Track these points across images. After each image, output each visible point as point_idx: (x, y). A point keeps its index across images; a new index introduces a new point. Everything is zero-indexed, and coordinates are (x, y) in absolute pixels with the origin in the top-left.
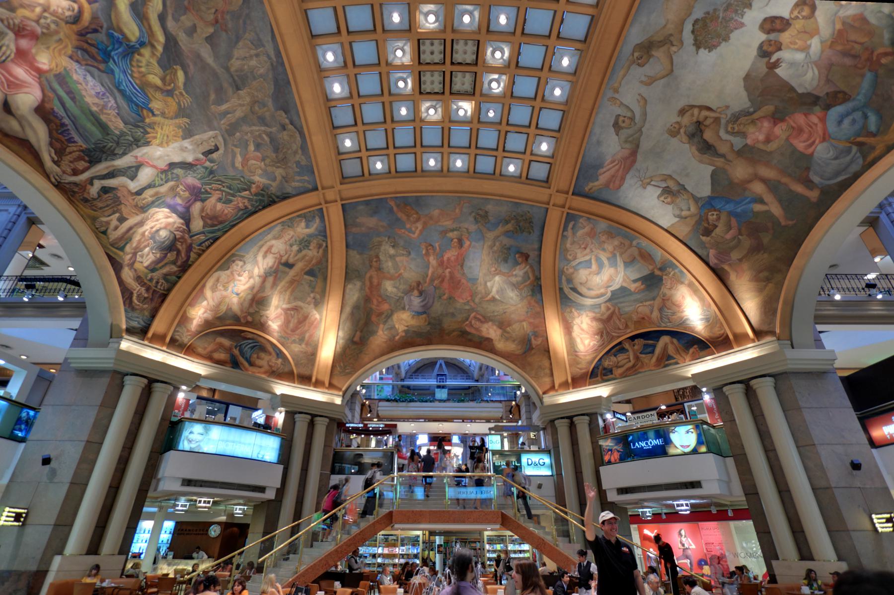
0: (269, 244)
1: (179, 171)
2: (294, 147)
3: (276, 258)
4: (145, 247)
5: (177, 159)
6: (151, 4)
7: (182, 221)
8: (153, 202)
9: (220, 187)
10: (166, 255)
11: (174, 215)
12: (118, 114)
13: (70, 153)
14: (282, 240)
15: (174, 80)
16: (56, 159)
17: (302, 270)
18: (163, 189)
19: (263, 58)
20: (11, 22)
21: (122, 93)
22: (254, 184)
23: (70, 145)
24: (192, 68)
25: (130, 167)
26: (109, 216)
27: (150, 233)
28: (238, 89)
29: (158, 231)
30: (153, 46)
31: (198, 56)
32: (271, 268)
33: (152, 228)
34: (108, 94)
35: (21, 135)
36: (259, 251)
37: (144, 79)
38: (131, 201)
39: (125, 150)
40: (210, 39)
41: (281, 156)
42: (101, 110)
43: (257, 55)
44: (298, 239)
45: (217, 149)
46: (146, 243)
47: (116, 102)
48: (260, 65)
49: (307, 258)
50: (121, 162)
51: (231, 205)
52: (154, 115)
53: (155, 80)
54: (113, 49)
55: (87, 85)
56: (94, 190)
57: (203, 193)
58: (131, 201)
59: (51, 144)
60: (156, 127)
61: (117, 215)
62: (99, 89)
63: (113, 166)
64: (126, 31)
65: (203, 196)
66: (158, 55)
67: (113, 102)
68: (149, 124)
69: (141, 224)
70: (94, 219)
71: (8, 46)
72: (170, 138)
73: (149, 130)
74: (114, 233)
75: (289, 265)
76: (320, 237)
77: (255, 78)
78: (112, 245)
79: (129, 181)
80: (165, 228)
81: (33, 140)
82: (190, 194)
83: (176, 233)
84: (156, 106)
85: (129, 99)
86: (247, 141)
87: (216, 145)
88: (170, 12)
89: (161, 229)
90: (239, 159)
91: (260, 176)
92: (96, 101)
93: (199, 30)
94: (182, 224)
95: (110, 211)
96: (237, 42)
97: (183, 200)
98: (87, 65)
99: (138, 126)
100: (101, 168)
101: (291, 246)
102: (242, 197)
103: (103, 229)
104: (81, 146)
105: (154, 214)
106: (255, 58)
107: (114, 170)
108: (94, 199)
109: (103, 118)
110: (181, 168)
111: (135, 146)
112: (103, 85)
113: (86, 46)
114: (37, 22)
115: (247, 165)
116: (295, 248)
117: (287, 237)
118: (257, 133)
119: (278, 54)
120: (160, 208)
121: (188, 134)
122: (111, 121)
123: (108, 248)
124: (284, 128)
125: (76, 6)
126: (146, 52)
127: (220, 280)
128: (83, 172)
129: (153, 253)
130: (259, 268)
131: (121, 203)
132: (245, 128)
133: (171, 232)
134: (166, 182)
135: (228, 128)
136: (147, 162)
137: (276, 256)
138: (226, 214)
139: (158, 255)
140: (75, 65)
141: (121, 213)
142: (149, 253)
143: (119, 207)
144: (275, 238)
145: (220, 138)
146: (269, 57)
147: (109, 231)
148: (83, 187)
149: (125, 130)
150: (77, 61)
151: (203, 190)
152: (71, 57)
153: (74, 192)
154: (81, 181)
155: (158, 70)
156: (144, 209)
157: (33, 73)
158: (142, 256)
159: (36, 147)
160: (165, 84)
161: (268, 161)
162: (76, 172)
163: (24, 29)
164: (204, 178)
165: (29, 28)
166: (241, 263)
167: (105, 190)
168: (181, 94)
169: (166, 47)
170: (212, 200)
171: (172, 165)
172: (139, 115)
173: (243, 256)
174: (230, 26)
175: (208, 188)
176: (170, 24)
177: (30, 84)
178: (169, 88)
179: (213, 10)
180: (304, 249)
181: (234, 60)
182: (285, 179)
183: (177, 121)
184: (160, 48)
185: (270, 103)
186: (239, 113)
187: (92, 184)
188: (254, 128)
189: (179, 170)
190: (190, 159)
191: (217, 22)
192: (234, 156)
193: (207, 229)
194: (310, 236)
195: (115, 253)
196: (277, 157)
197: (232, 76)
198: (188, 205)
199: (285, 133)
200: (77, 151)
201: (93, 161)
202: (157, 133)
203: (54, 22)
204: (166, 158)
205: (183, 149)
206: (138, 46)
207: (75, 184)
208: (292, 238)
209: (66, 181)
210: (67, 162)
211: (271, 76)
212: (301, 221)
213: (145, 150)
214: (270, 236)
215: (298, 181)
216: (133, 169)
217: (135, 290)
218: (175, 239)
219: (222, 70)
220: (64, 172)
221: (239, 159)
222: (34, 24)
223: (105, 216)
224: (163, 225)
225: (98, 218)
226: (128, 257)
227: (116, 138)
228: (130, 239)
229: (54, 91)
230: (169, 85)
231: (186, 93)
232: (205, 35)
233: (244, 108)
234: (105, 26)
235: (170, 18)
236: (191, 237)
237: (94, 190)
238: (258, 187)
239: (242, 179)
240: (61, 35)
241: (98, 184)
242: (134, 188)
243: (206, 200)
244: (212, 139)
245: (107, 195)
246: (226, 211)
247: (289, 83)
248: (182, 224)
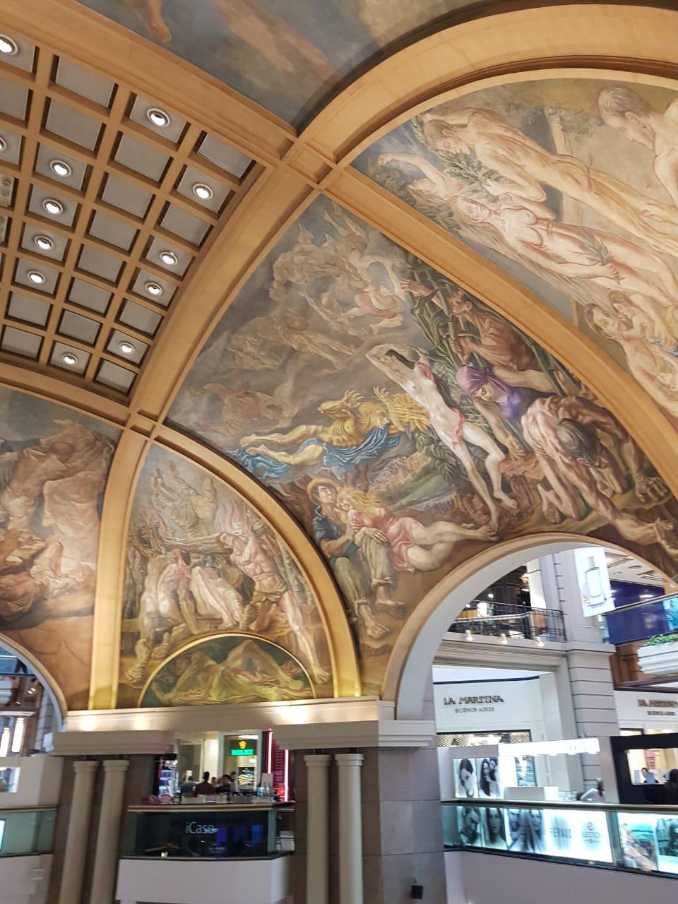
0: (521, 249)
1: (455, 395)
2: (298, 259)
3: (549, 233)
4: (589, 474)
5: (438, 398)
6: (279, 442)
7: (537, 402)
8: (514, 435)
9: (451, 341)
10: (602, 446)
11: (529, 411)
12: (407, 457)
13: (465, 509)
14: (493, 220)
15: (339, 411)
16: (472, 525)
17: (545, 162)
18: (492, 420)
19: (234, 342)
20: (354, 527)
21: (381, 453)
22: (411, 294)
23: (456, 506)
24: (312, 398)
25: (469, 450)
26: (541, 498)
27: (566, 456)
28: (293, 351)
29: (560, 442)
30: (315, 433)
31: (294, 397)
32: (582, 246)
33: (557, 450)
34: (389, 464)
35: (451, 546)
36: (551, 272)
37: (354, 435)
38: (518, 463)
39: (449, 454)
40: (269, 391)
41: (331, 270)
42: (410, 471)
43: (240, 350)
44: (467, 187)
45: (391, 353)
46: (583, 470)
47: (395, 457)
48: (247, 343)
49: (501, 152)
50: (467, 462)
51: (477, 322)
52: (391, 423)
53: (349, 426)
54: (341, 461)
55: (387, 481)
56: (508, 502)
57: (476, 363)
58: (518, 463)
59: (459, 523)
60: (406, 421)
61: (540, 487)
62: (386, 470)
63: (473, 471)
64: (317, 454)
65: (482, 366)
66: (320, 428)
67: (395, 460)
68: (405, 427)
69: (551, 462)
70: (543, 520)
71: (375, 533)
72: (411, 406)
73: (413, 428)
74: (564, 505)
75: (553, 200)
76: (420, 136)
77: (265, 341)
78: (581, 518)
79: (489, 457)
80: (555, 430)
81: (454, 538)
82: (487, 382)
83: (561, 417)
84: (379, 421)
85: (385, 447)
86: (350, 320)
87: (387, 354)
88: (273, 428)
89: (557, 437)
90: (385, 322)
91: (391, 288)
92: (400, 473)
93: (270, 403)
94: (543, 403)
95: (535, 494)
96: (247, 371)
97: (500, 395)
98: (367, 480)
99: (413, 437)
100: (479, 484)
101: (495, 199)
102: (449, 307)
103: (557, 515)
104: (456, 497)
105: (533, 439)
106: (245, 350)
107: (478, 471)
108: (519, 506)
109: (418, 471)
110: (449, 394)
111: (440, 444)
112: (381, 469)
113: (349, 481)
114: (347, 511)
115: (387, 310)
116: (494, 188)
117: (480, 214)
118: (329, 311)
119: (215, 335)
120: (522, 428)
121: (393, 388)
122: (418, 463)
123: (585, 526)
124: (288, 285)
125: (320, 487)
126: (326, 437)
127: (649, 371)
128: (485, 504)
129: (600, 467)
130: (595, 277)
131: (523, 476)
132: (335, 327)
133: (561, 423)
134: (479, 413)
135: (352, 346)
136: (457, 432)
137: (544, 234)
138: (498, 330)
139: (605, 461)
140: (371, 488)
141: (539, 482)
142: (599, 472)
143: (529, 481)
144: (498, 237)
145: (374, 351)
146: (229, 340)
147: (561, 509)
148: (504, 512)
149: (424, 451)
150: (367, 486)
151: (471, 365)
152: (366, 491)
153: (509, 524)
154: (496, 510)
155: (336, 425)
156: (528, 453)
157: (391, 520)
158: (605, 487)
159: (462, 538)
160: (348, 417)
161: (359, 285)
162: (487, 512)
163: (356, 520)
164: (449, 364)
165: (354, 517)
166: (598, 316)
167: (506, 488)
168: (347, 401)
169: (308, 423)
170: (482, 351)
171: (450, 403)
172: (399, 437)
173: (579, 307)
174: (239, 382)
175: (463, 359)
176: (284, 424)
177: (401, 525)
178: (349, 413)
179: (241, 399)
180: (480, 167)
181: (267, 366)
182: (362, 248)
183: (384, 400)
184: (313, 428)
185: (276, 313)
186: (322, 339)
187: (500, 501)
188: (325, 317)
189: (452, 395)
190: (429, 383)
191: (247, 394)
192: (387, 330)
193: (541, 365)
194: (435, 161)
195: (592, 522)
196: (338, 276)
197: (286, 361)
198: (505, 388)
199: (293, 280)
200: (462, 501)
201: (473, 492)
202: (413, 419)
203: (341, 500)
204: (442, 410)
205: (419, 390)
206: (324, 444)
207: (500, 518)
208: (473, 202)
209: (497, 525)
210: (476, 516)
211: (245, 328)
212: (418, 193)
213: (441, 433)
214: (502, 250)
215: (346, 228)
216: (472, 449)
217: (655, 537)
218: (573, 421)
219: (288, 371)
220: (487, 523)
221: (385, 322)
222: (349, 514)
223: (541, 504)
224: (550, 432)
225: (543, 514)
226: (601, 507)
227: (438, 462)
228: (575, 488)
229: (402, 507)
230: (346, 413)
231: (344, 396)
232: (269, 397)
233: (310, 336)
234: (322, 468)
235: (278, 426)
236: (564, 395)
237: (508, 502)
238: (410, 286)
239: (417, 312)
240: (350, 497)
241: (499, 494)
242: (499, 454)
243: (487, 362)
244: (382, 359)
245: (513, 488)
246: (491, 330)
247: (231, 308)
248: (543, 403)
